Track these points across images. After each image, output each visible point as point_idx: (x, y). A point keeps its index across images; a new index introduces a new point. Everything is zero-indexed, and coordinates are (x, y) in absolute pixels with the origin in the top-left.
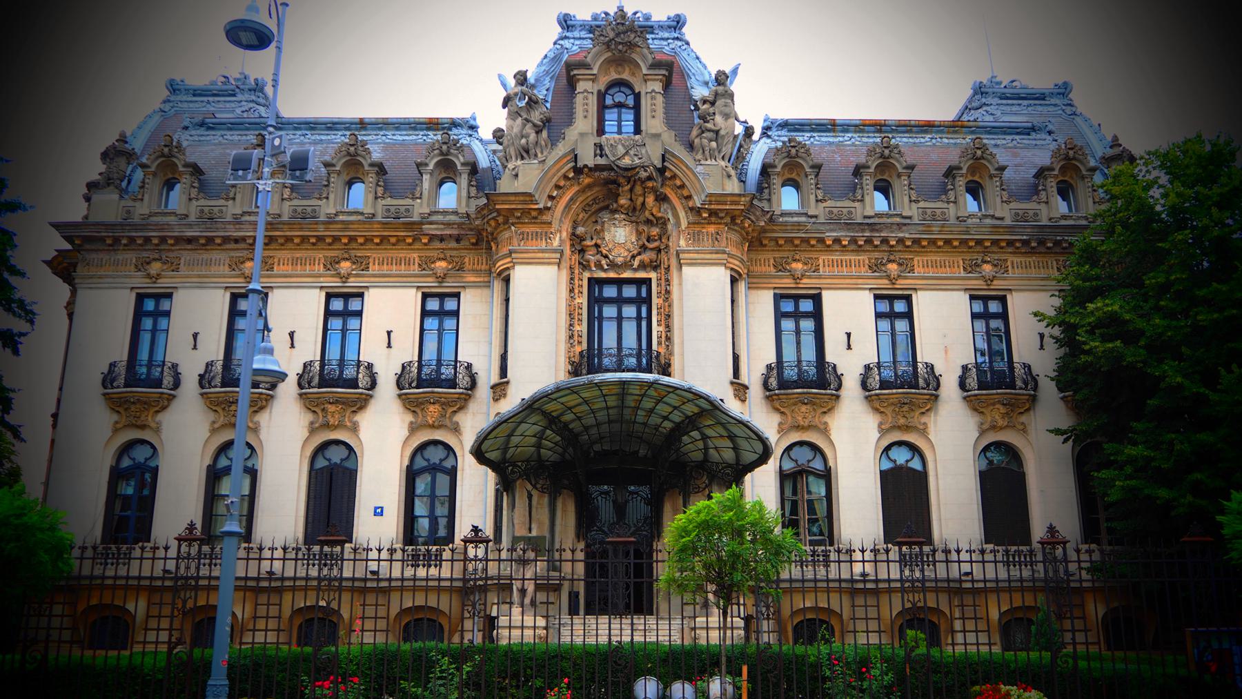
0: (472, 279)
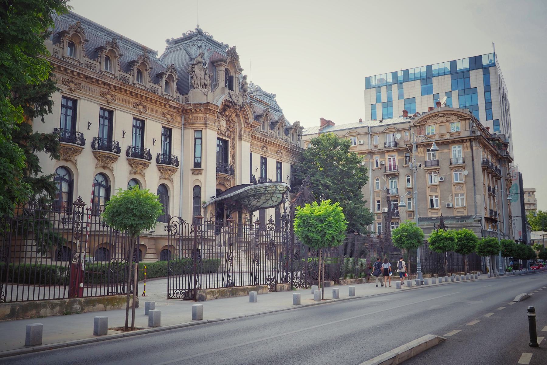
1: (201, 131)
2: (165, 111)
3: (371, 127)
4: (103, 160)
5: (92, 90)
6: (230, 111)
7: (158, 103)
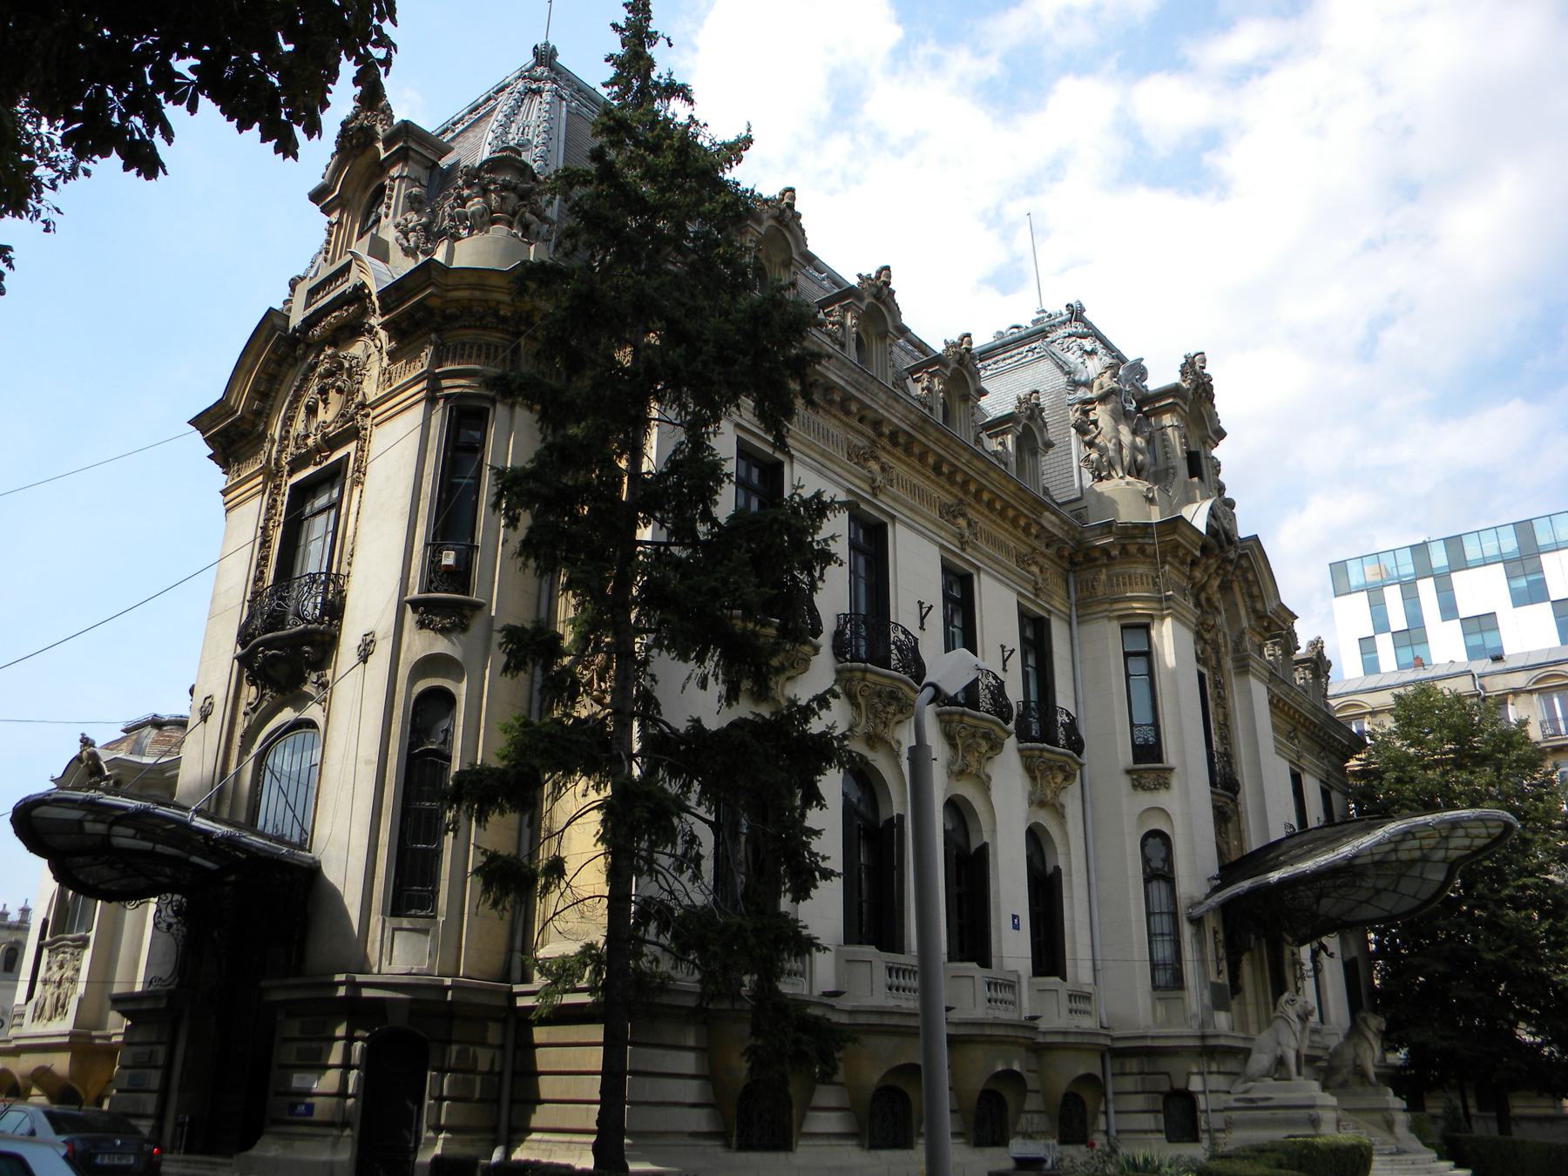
0: (1058, 605)
1: (1146, 628)
2: (1025, 550)
3: (1481, 676)
4: (871, 707)
5: (826, 436)
6: (1206, 569)
7: (1011, 513)
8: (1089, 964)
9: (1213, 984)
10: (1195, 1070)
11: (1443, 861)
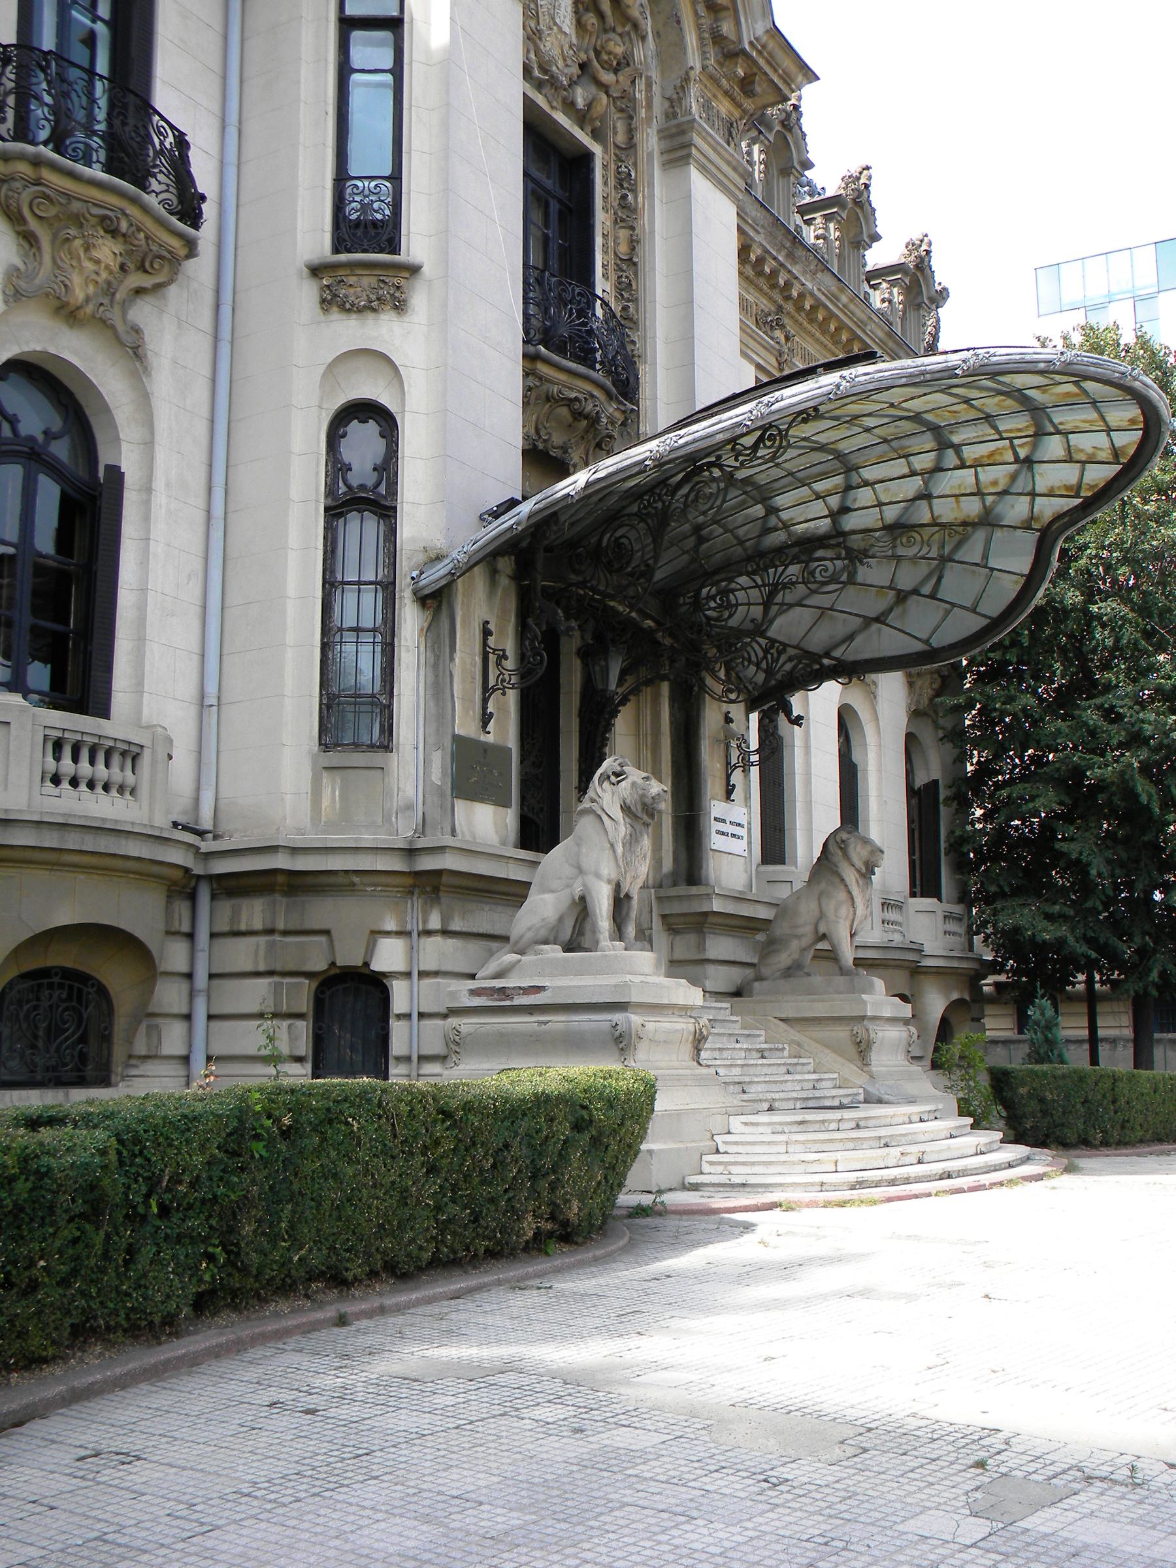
8: (187, 688)
9: (457, 739)
10: (391, 925)
11: (1027, 526)
